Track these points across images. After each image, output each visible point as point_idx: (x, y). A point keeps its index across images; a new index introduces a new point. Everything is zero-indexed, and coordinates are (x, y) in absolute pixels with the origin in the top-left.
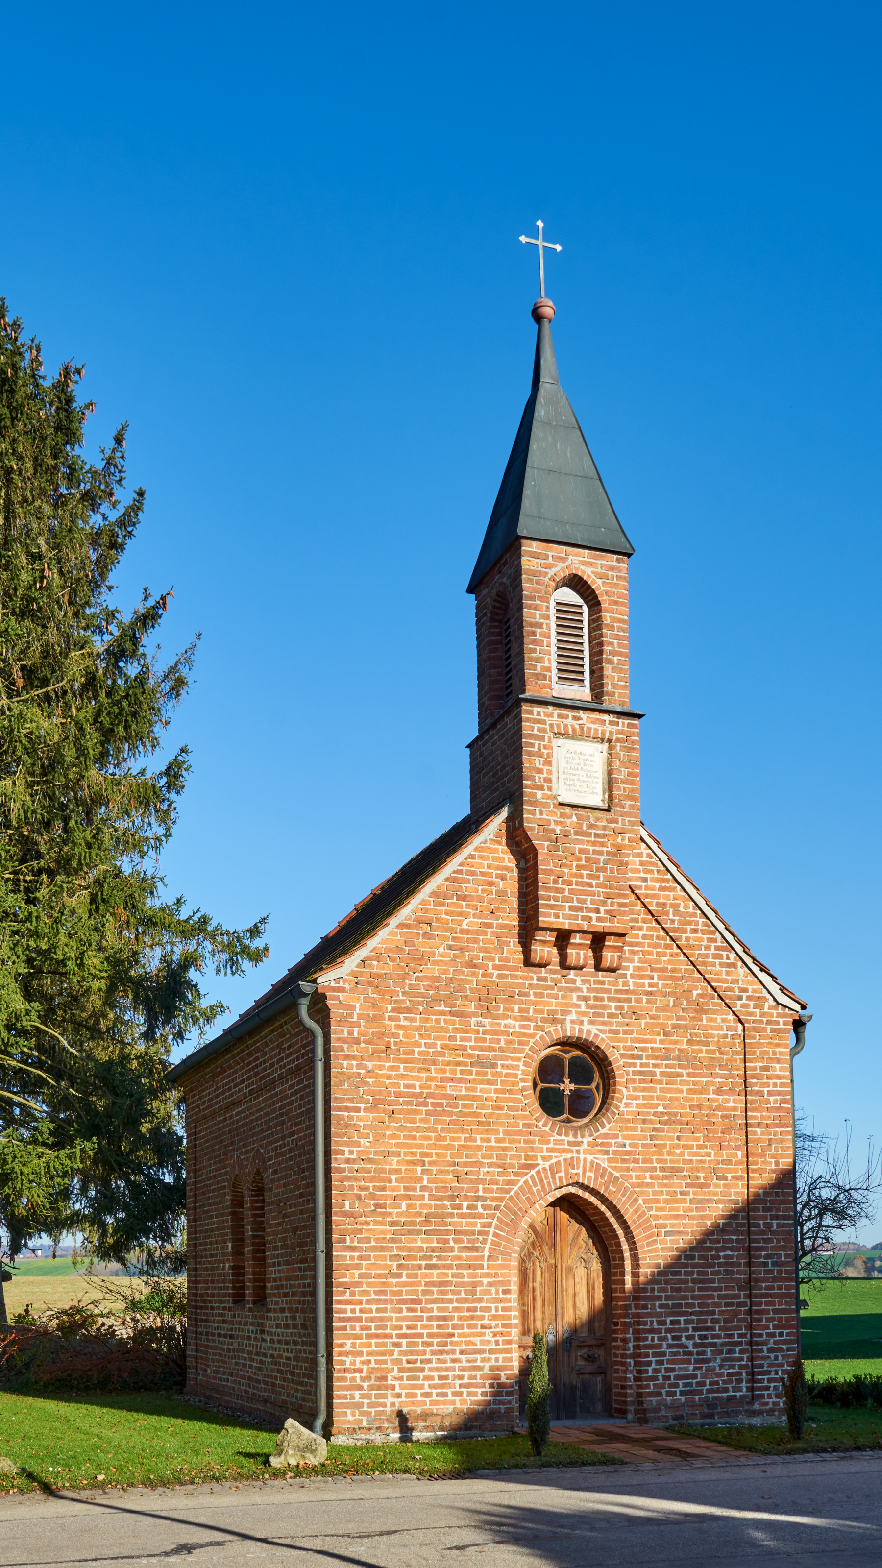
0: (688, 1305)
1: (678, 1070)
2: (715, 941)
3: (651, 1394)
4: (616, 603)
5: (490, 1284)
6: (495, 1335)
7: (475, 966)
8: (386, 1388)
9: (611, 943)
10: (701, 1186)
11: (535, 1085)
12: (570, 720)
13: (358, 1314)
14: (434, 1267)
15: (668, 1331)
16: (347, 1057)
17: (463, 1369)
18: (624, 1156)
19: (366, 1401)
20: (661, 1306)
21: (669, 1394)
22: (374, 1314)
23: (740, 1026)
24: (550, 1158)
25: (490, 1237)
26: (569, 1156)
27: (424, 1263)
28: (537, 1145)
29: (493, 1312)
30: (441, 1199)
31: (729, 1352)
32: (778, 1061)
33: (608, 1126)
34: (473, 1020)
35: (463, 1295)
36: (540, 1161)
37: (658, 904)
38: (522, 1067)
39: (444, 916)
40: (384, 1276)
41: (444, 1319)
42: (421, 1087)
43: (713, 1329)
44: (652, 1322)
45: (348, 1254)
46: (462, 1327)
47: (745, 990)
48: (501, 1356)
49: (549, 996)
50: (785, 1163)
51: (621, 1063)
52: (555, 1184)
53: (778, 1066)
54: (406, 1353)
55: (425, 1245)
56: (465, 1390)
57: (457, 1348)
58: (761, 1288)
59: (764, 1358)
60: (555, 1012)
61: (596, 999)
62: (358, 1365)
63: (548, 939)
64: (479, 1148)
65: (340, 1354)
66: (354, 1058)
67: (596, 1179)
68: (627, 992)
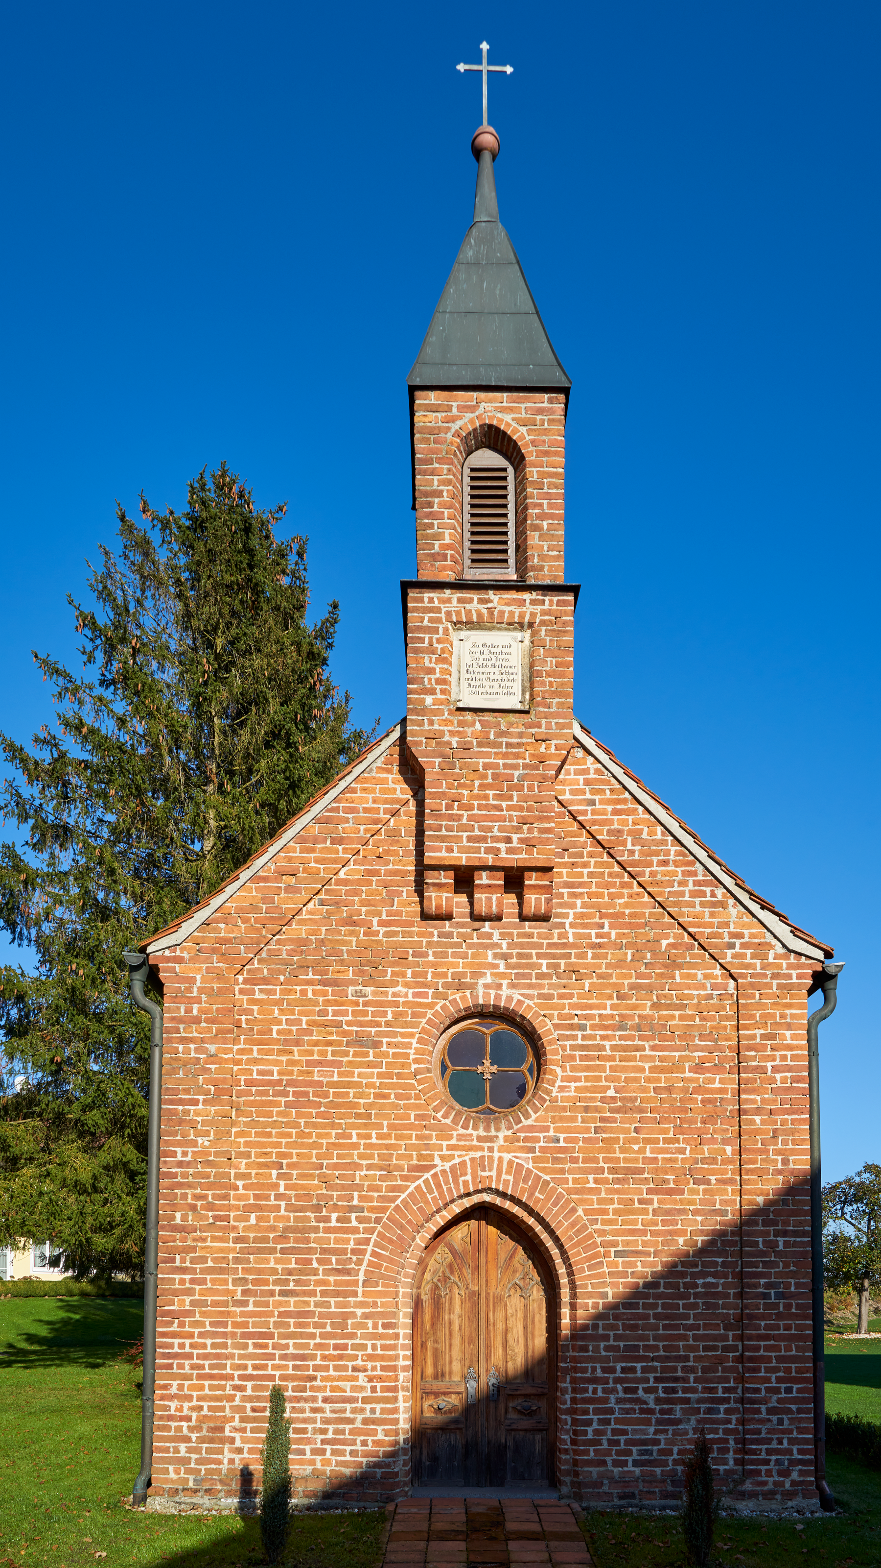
0: (647, 1348)
1: (637, 1042)
2: (695, 874)
3: (590, 1463)
4: (546, 453)
5: (366, 1316)
6: (370, 1380)
7: (355, 923)
8: (222, 1441)
9: (533, 882)
10: (670, 1192)
11: (444, 1068)
12: (475, 604)
13: (187, 1349)
14: (291, 1293)
15: (617, 1381)
16: (183, 1040)
17: (327, 1421)
18: (555, 1154)
19: (194, 1456)
20: (607, 1349)
21: (616, 1463)
22: (209, 1350)
23: (732, 983)
24: (452, 1157)
25: (368, 1256)
26: (479, 1154)
27: (277, 1288)
28: (434, 1141)
29: (369, 1351)
30: (302, 1209)
31: (709, 1411)
32: (789, 1027)
33: (534, 1116)
34: (351, 990)
35: (328, 1329)
36: (437, 1161)
37: (609, 832)
38: (415, 1045)
40: (225, 1304)
41: (303, 1357)
42: (279, 1073)
43: (685, 1380)
44: (594, 1369)
45: (177, 1277)
46: (327, 1368)
47: (740, 936)
48: (378, 1407)
49: (454, 955)
50: (801, 1163)
51: (555, 1035)
52: (458, 1189)
53: (788, 1033)
54: (250, 1399)
55: (280, 1267)
56: (328, 1448)
57: (320, 1395)
58: (758, 1327)
59: (762, 1421)
60: (464, 975)
61: (520, 956)
62: (186, 1412)
63: (444, 881)
64: (355, 1146)
65: (162, 1398)
66: (192, 1040)
67: (516, 1183)
68: (564, 945)
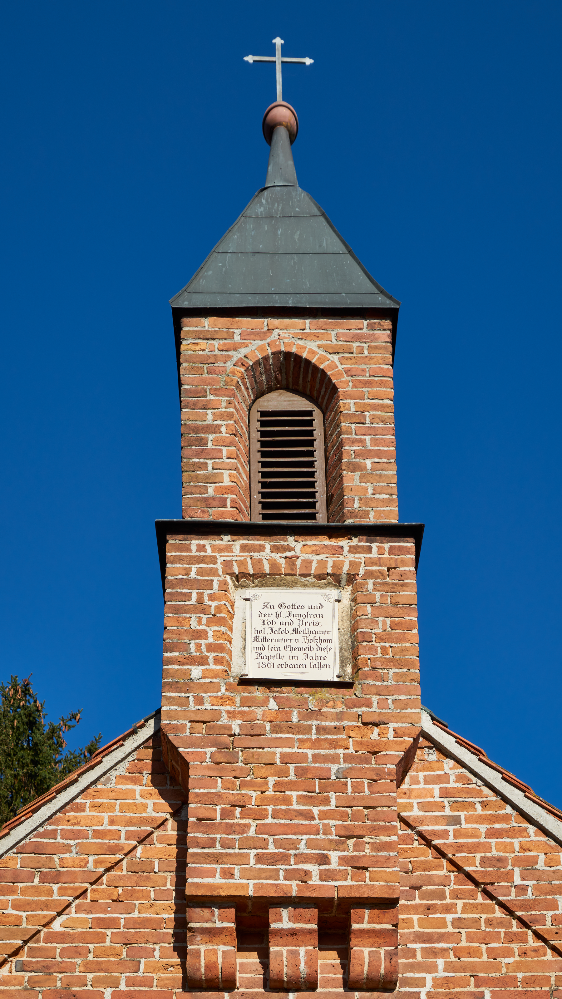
4: (367, 384)
9: (365, 926)
39: (9, 911)
63: (219, 924)
